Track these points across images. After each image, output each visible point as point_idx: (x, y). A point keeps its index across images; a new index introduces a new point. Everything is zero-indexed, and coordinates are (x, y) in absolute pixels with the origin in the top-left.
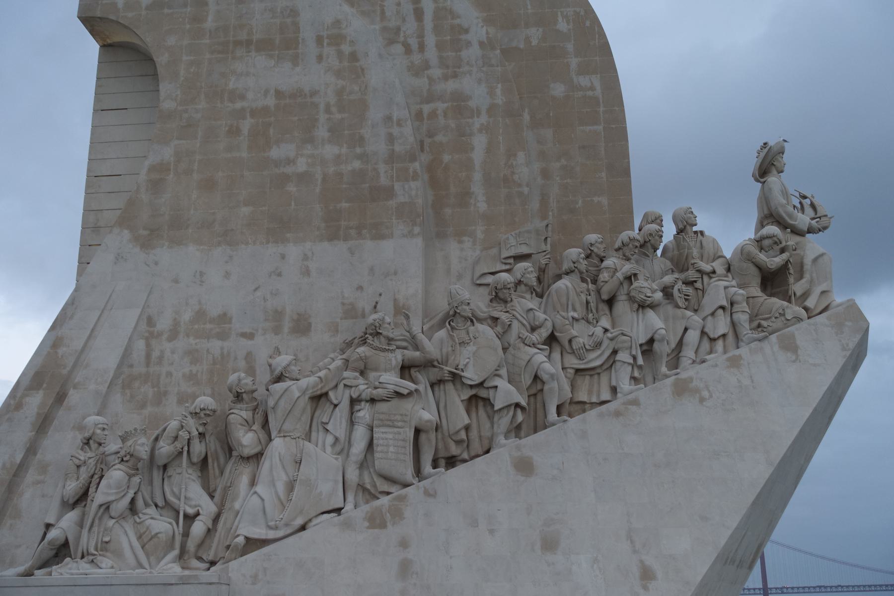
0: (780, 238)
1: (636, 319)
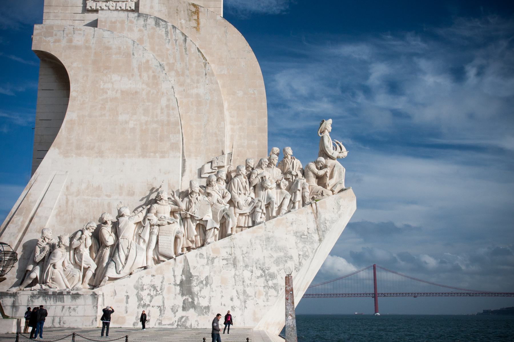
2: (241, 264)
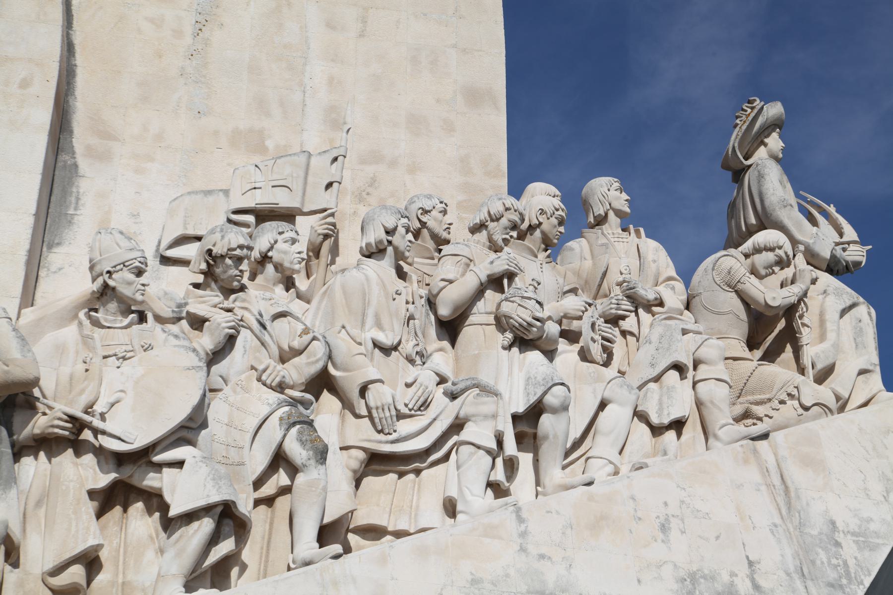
0: (789, 253)
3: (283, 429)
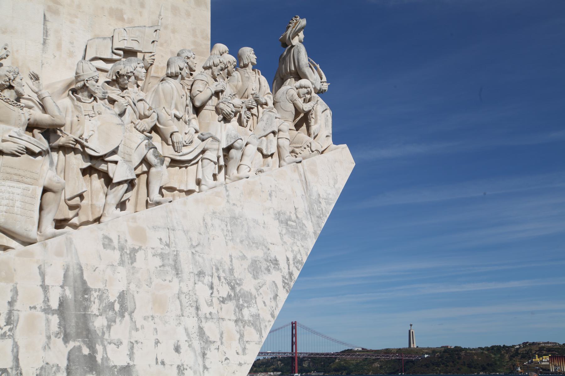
1: (219, 128)
2: (187, 267)
3: (147, 150)
